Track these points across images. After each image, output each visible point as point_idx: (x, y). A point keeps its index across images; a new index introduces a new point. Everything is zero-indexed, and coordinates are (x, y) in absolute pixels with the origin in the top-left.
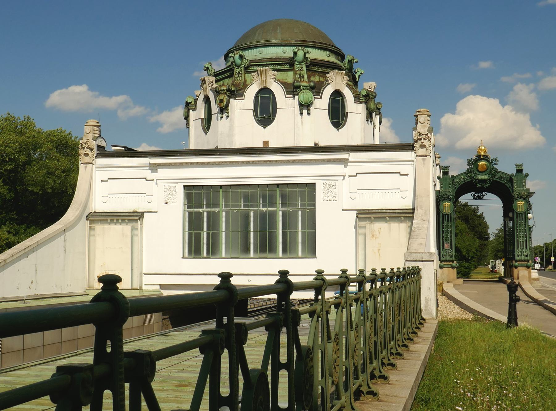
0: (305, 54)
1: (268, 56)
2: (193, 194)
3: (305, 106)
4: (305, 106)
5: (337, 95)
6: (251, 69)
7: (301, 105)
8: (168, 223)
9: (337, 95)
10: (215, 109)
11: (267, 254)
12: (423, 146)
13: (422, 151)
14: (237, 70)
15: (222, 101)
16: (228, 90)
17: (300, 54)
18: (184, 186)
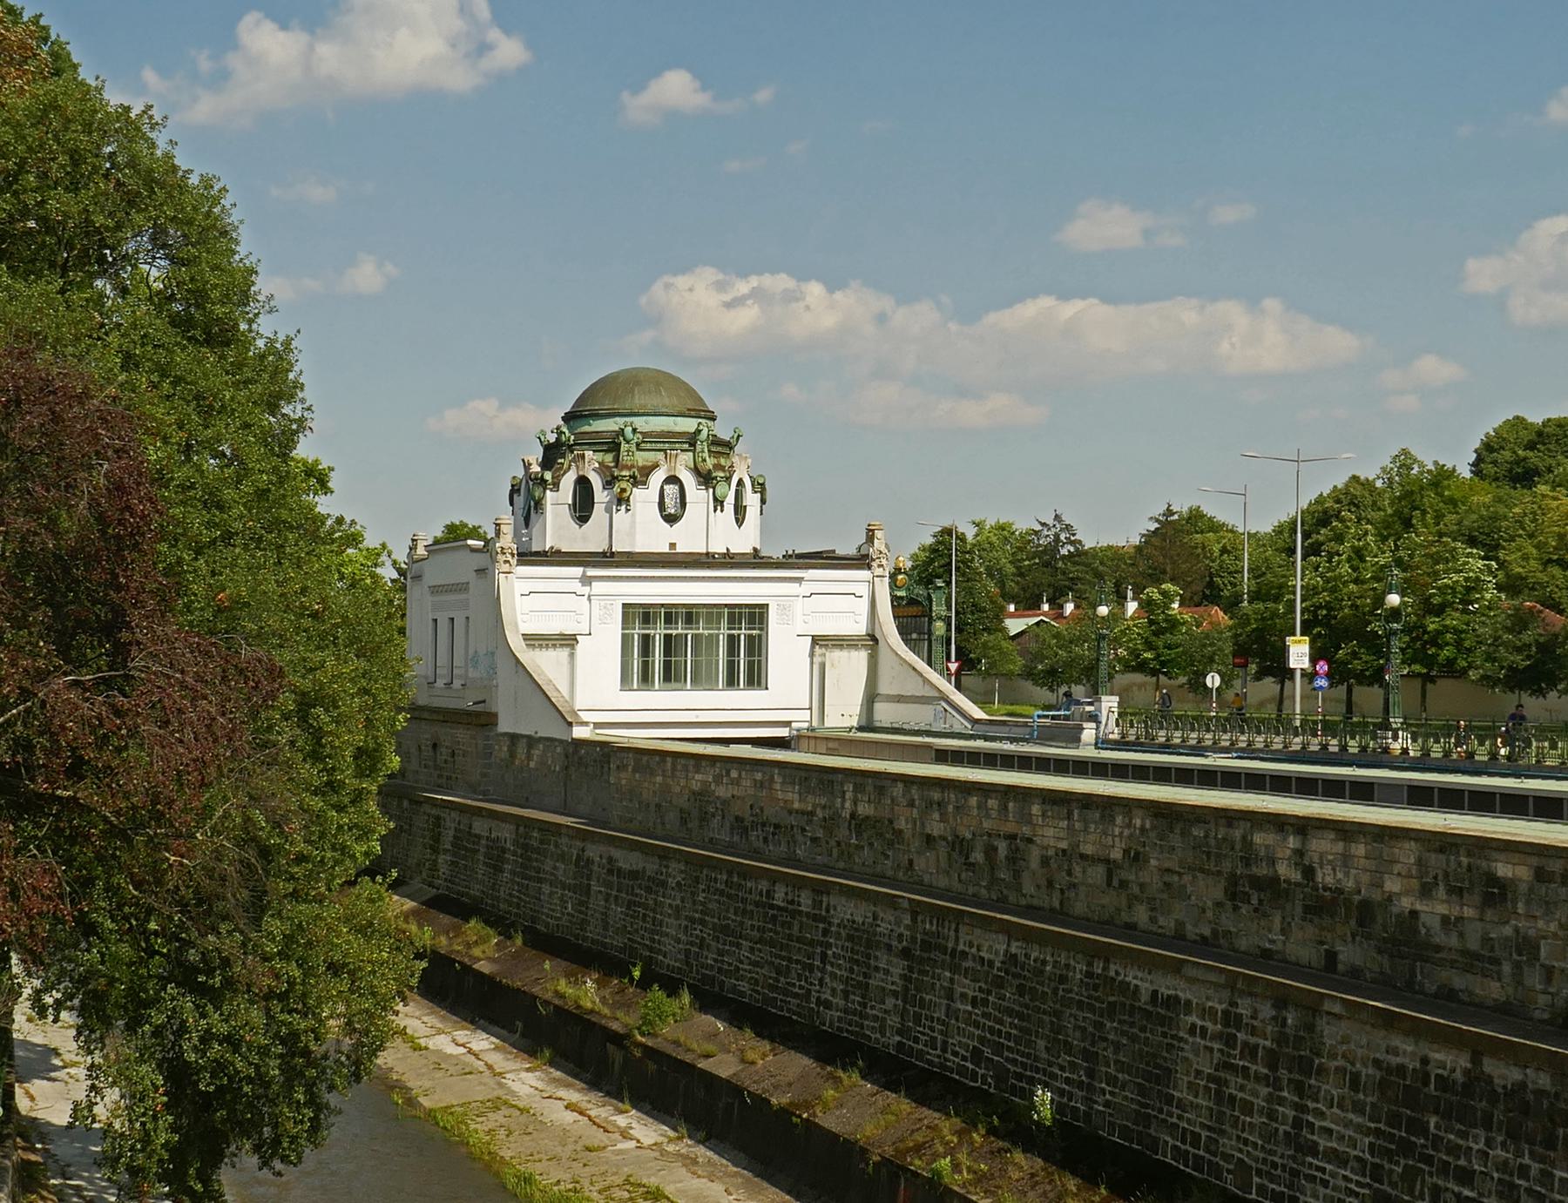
1: (658, 429)
3: (719, 503)
4: (719, 503)
5: (740, 483)
6: (643, 446)
7: (715, 499)
8: (604, 646)
9: (740, 483)
10: (601, 496)
11: (674, 685)
12: (880, 566)
13: (879, 571)
14: (624, 447)
15: (624, 490)
16: (633, 477)
18: (624, 605)
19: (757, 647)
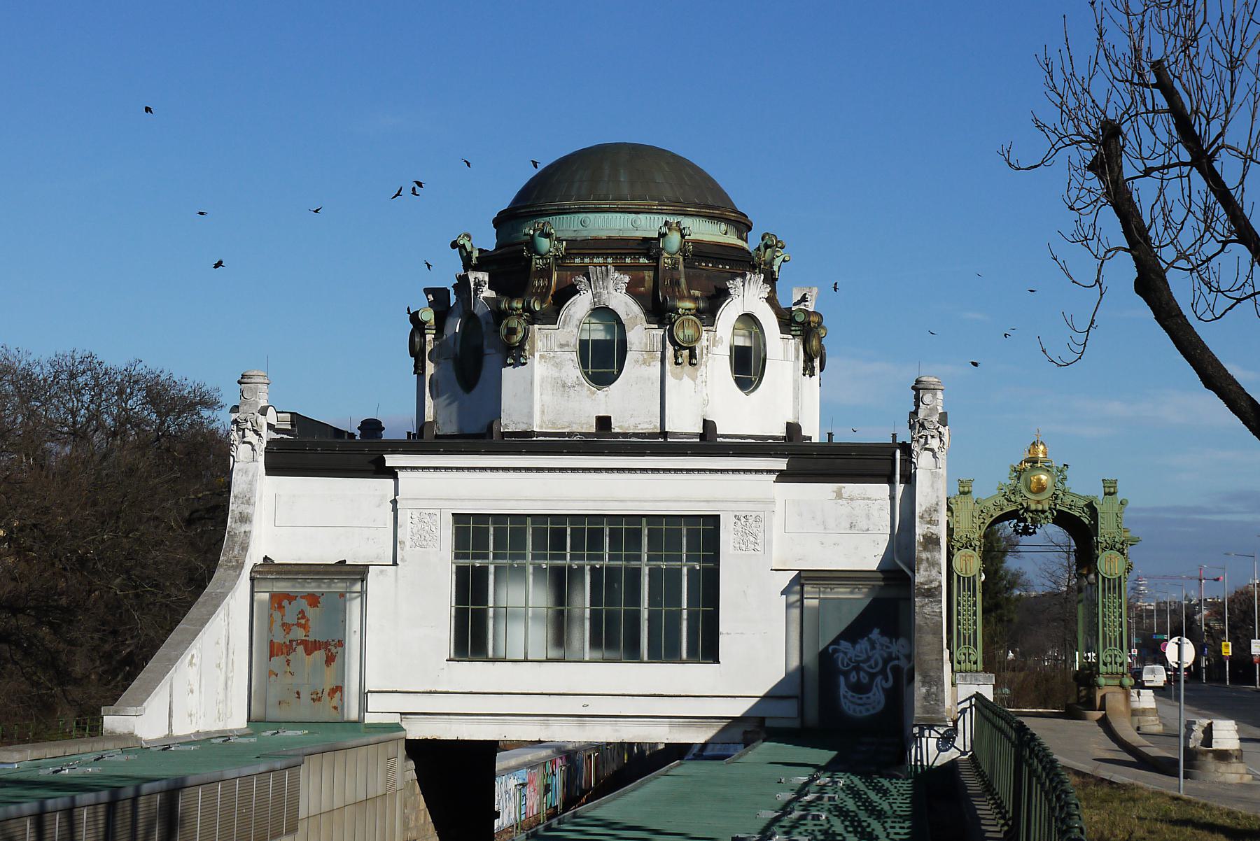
0: (683, 236)
1: (603, 235)
2: (472, 531)
15: (512, 331)
18: (457, 517)
19: (708, 588)
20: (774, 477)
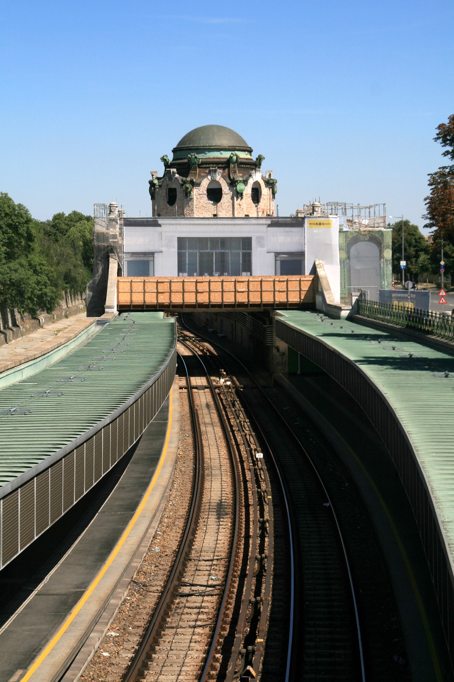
2: (182, 242)
17: (235, 158)
20: (267, 226)
